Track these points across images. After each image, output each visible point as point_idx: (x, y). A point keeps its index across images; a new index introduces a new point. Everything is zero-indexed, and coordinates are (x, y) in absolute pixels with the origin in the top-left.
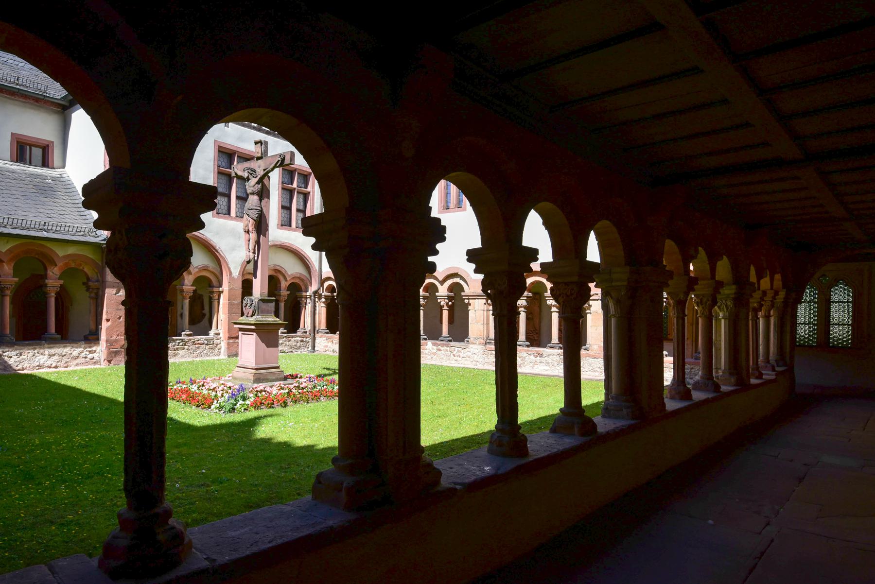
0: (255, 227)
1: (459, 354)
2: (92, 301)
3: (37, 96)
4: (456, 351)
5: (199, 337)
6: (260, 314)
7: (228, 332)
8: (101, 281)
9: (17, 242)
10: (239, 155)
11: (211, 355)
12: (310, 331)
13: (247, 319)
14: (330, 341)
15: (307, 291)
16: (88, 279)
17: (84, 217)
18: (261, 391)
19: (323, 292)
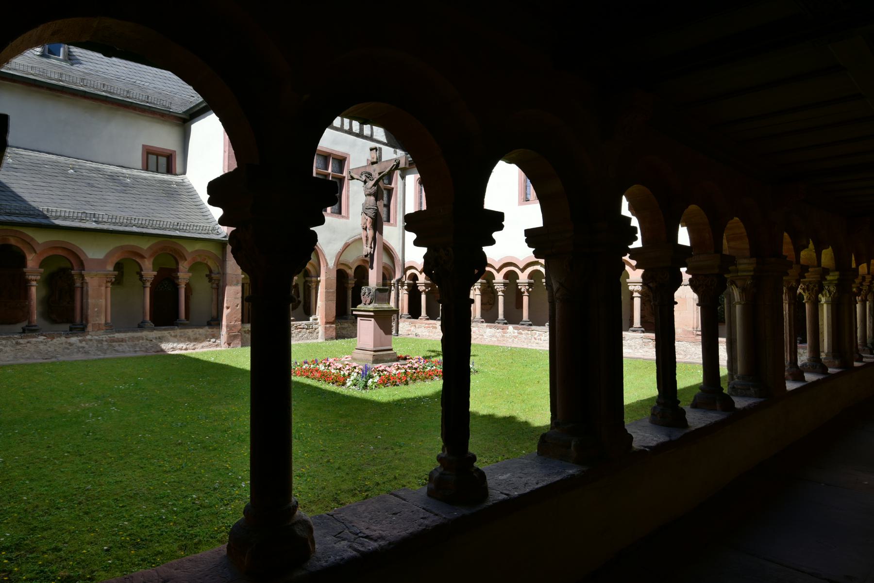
0: (372, 225)
1: (541, 337)
2: (214, 291)
3: (162, 111)
4: (537, 334)
5: (300, 322)
6: (376, 302)
7: (326, 318)
8: (222, 273)
9: (153, 241)
10: (334, 157)
11: (310, 338)
13: (365, 306)
15: (391, 280)
16: (211, 271)
17: (206, 217)
18: (382, 371)
19: (406, 280)
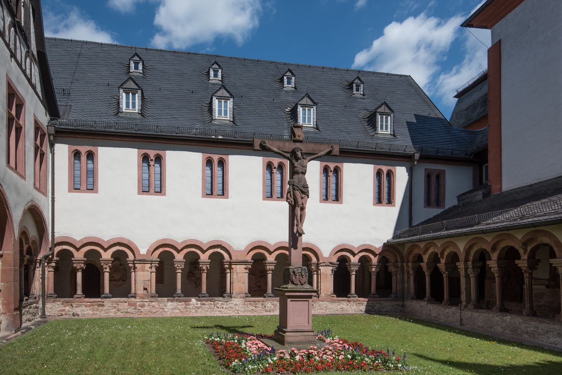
1: (223, 306)
4: (220, 304)
12: (39, 296)
14: (68, 305)
